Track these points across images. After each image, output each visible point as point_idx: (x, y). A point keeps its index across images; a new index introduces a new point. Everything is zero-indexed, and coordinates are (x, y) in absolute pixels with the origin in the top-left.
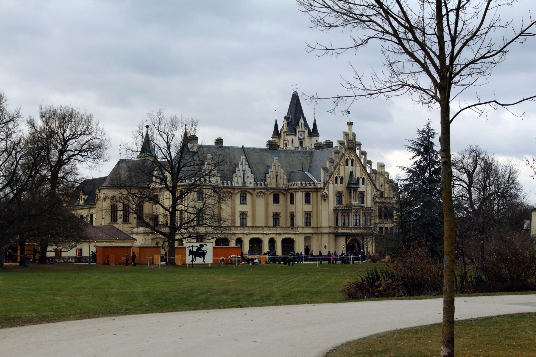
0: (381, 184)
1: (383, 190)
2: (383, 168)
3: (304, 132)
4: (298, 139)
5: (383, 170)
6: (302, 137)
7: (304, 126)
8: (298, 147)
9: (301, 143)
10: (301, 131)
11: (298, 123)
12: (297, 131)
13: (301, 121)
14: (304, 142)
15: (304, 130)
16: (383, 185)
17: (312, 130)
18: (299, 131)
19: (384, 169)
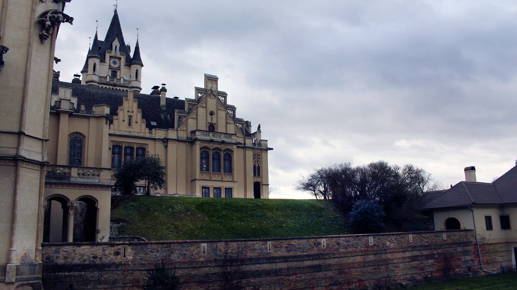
0: (209, 111)
1: (214, 121)
2: (214, 83)
3: (120, 59)
4: (108, 66)
5: (215, 86)
6: (116, 66)
7: (120, 50)
8: (105, 76)
9: (114, 73)
10: (115, 57)
11: (111, 46)
12: (108, 56)
13: (116, 43)
14: (118, 73)
15: (118, 55)
16: (215, 112)
17: (132, 56)
18: (111, 57)
19: (217, 84)
